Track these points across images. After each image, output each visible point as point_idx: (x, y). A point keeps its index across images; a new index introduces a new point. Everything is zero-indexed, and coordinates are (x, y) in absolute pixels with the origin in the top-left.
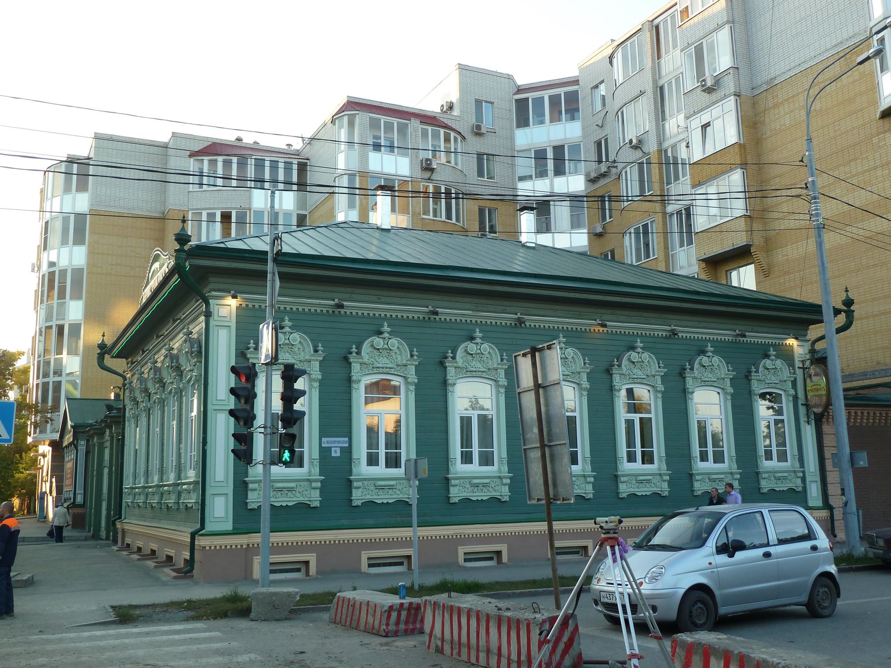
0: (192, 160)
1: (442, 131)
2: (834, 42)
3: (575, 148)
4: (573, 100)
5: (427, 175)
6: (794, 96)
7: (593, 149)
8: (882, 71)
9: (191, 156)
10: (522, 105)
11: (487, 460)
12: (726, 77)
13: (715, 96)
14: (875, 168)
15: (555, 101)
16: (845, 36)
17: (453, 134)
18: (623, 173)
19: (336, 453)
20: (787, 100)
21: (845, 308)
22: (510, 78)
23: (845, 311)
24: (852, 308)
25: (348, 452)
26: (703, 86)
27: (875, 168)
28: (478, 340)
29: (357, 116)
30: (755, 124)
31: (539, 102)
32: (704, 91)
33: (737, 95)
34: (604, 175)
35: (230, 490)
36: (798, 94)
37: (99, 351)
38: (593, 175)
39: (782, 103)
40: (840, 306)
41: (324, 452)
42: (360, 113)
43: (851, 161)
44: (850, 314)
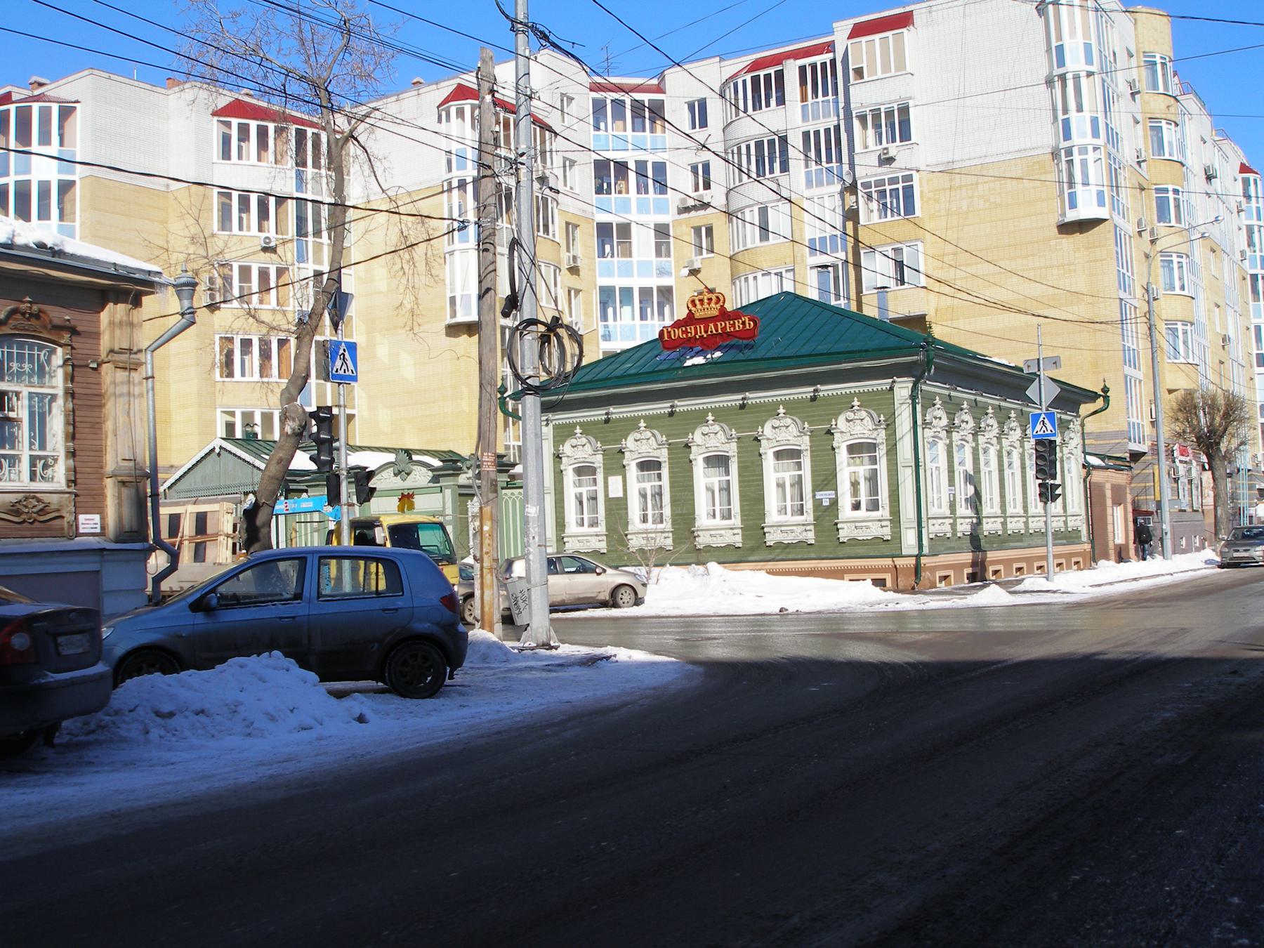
0: (216, 118)
2: (1017, 148)
9: (214, 114)
11: (801, 511)
14: (1052, 267)
16: (1029, 145)
18: (747, 211)
20: (965, 186)
21: (1102, 394)
23: (1104, 397)
24: (1108, 394)
27: (1052, 267)
31: (618, 104)
37: (499, 396)
43: (1028, 256)
44: (1106, 399)
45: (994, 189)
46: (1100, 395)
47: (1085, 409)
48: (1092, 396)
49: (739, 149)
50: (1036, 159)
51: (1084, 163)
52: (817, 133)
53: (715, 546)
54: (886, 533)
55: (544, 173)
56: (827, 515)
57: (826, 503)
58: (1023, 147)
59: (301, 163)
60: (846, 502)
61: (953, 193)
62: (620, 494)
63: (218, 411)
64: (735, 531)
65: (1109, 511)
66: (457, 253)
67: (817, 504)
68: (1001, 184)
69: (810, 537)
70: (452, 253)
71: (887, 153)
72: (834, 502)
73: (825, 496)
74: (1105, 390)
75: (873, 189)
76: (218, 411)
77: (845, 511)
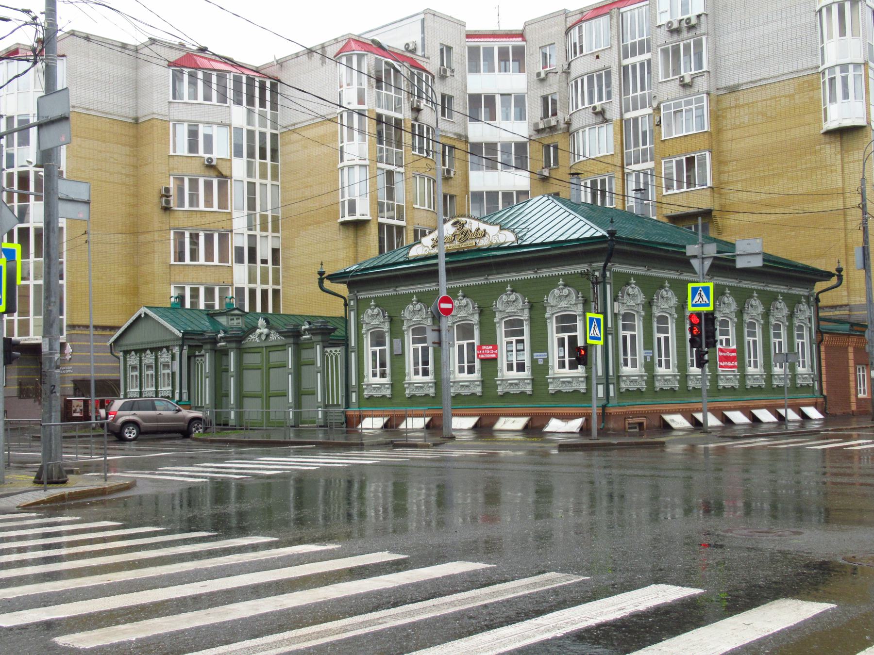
1: (424, 74)
2: (791, 70)
3: (520, 100)
4: (519, 54)
5: (415, 115)
6: (753, 103)
7: (539, 103)
8: (831, 101)
9: (169, 66)
10: (473, 52)
12: (700, 78)
13: (688, 91)
15: (503, 53)
16: (800, 68)
17: (430, 77)
18: (581, 131)
19: (648, 360)
20: (746, 104)
21: (837, 273)
22: (462, 24)
23: (837, 275)
24: (842, 273)
25: (652, 358)
26: (681, 81)
28: (633, 285)
29: (365, 57)
30: (718, 117)
31: (489, 51)
32: (680, 85)
33: (708, 94)
34: (552, 129)
35: (615, 381)
36: (757, 102)
37: (319, 277)
38: (541, 126)
39: (743, 106)
40: (834, 271)
41: (645, 357)
42: (369, 54)
44: (840, 278)
45: (771, 106)
46: (833, 275)
47: (819, 286)
48: (828, 275)
49: (576, 83)
50: (805, 79)
51: (845, 80)
52: (634, 67)
53: (564, 391)
54: (582, 387)
55: (418, 106)
56: (540, 370)
57: (541, 362)
58: (795, 69)
59: (250, 102)
60: (554, 361)
61: (737, 111)
62: (400, 352)
63: (172, 287)
64: (476, 383)
65: (852, 370)
66: (346, 169)
67: (534, 361)
68: (776, 101)
69: (528, 389)
70: (342, 169)
71: (683, 81)
72: (546, 361)
73: (540, 356)
74: (839, 270)
75: (672, 111)
76: (172, 287)
77: (555, 371)
